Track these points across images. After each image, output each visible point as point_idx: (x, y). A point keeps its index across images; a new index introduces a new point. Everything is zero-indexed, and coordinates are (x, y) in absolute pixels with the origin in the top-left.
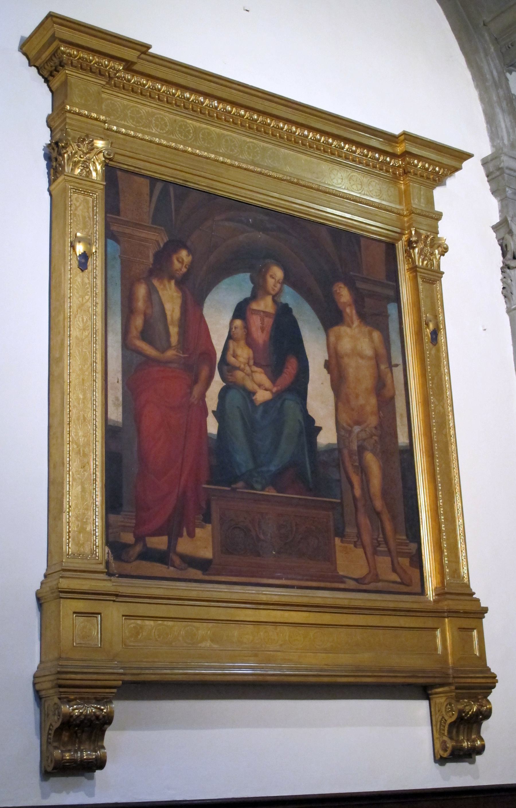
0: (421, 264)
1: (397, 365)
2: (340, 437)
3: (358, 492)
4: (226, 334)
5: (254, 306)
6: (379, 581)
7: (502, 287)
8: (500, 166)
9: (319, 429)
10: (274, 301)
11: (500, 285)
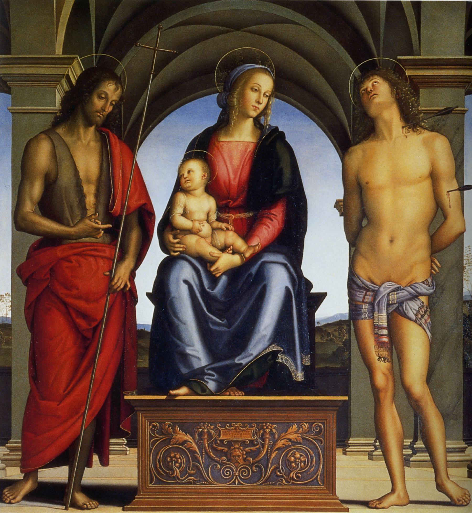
9: (321, 297)
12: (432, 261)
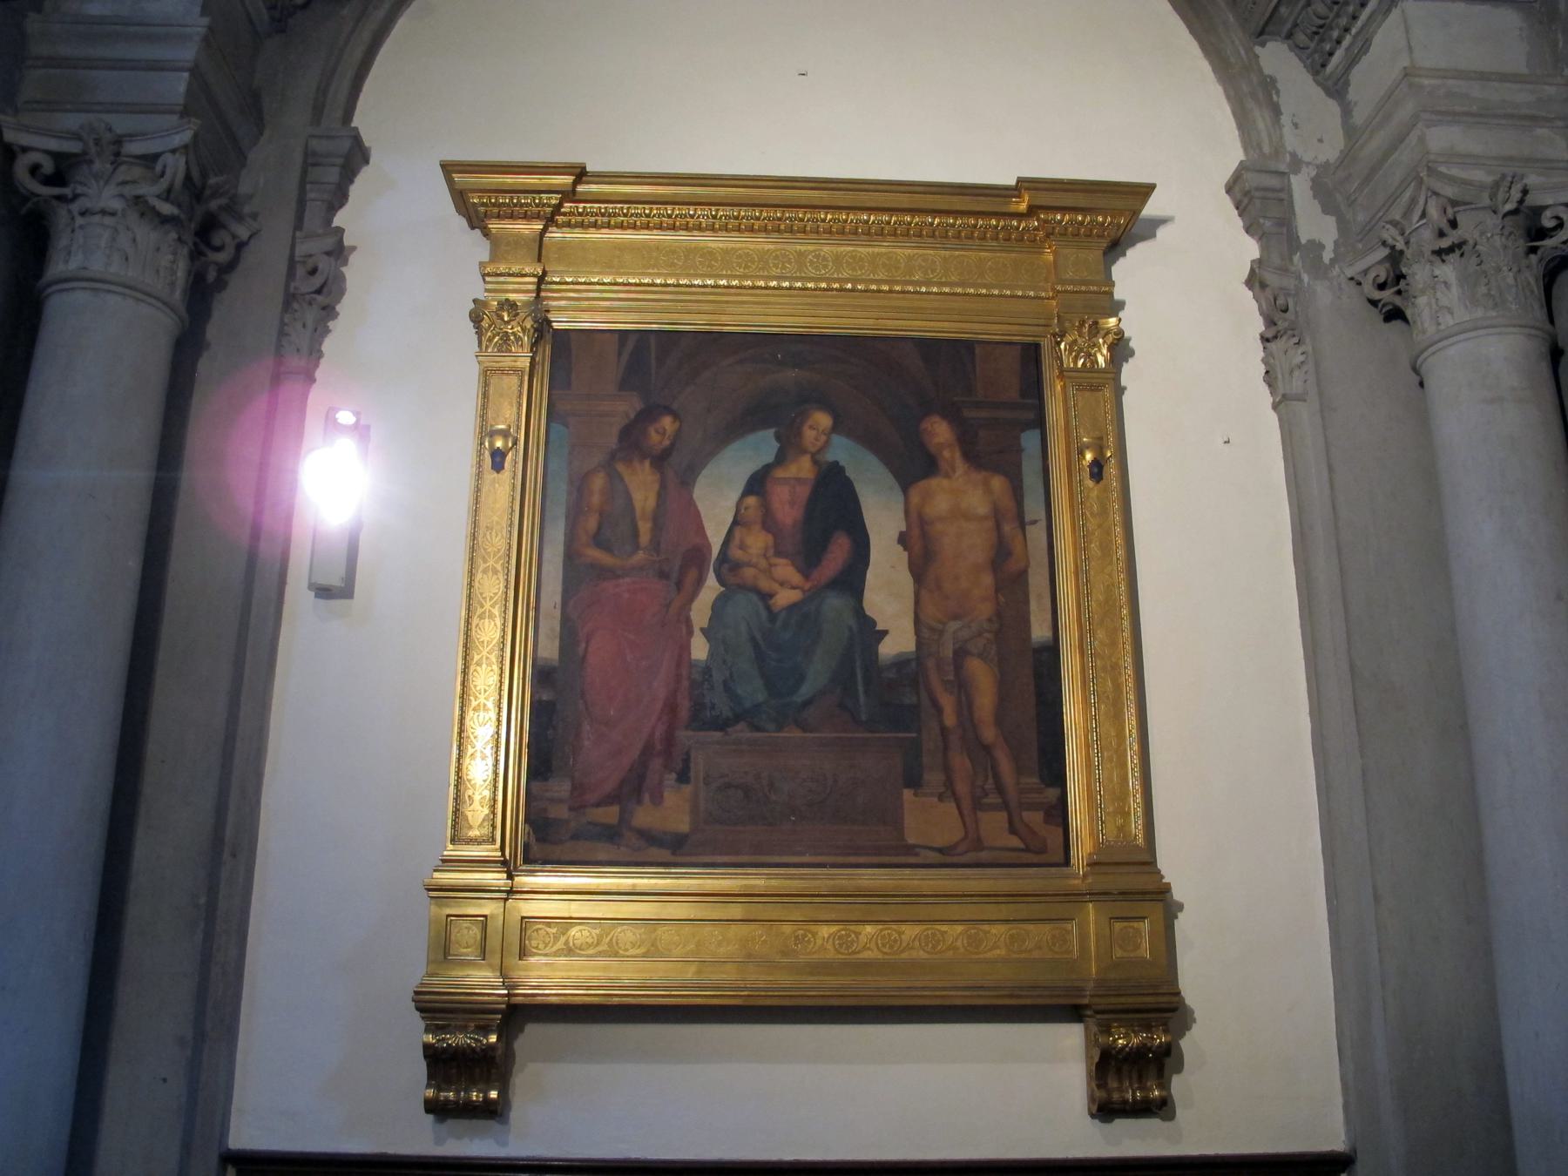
0: (1072, 365)
1: (1034, 522)
2: (919, 644)
3: (950, 719)
4: (730, 519)
5: (780, 473)
6: (983, 849)
7: (1265, 371)
8: (1246, 189)
9: (885, 633)
10: (815, 462)
11: (1262, 369)
12: (997, 598)
